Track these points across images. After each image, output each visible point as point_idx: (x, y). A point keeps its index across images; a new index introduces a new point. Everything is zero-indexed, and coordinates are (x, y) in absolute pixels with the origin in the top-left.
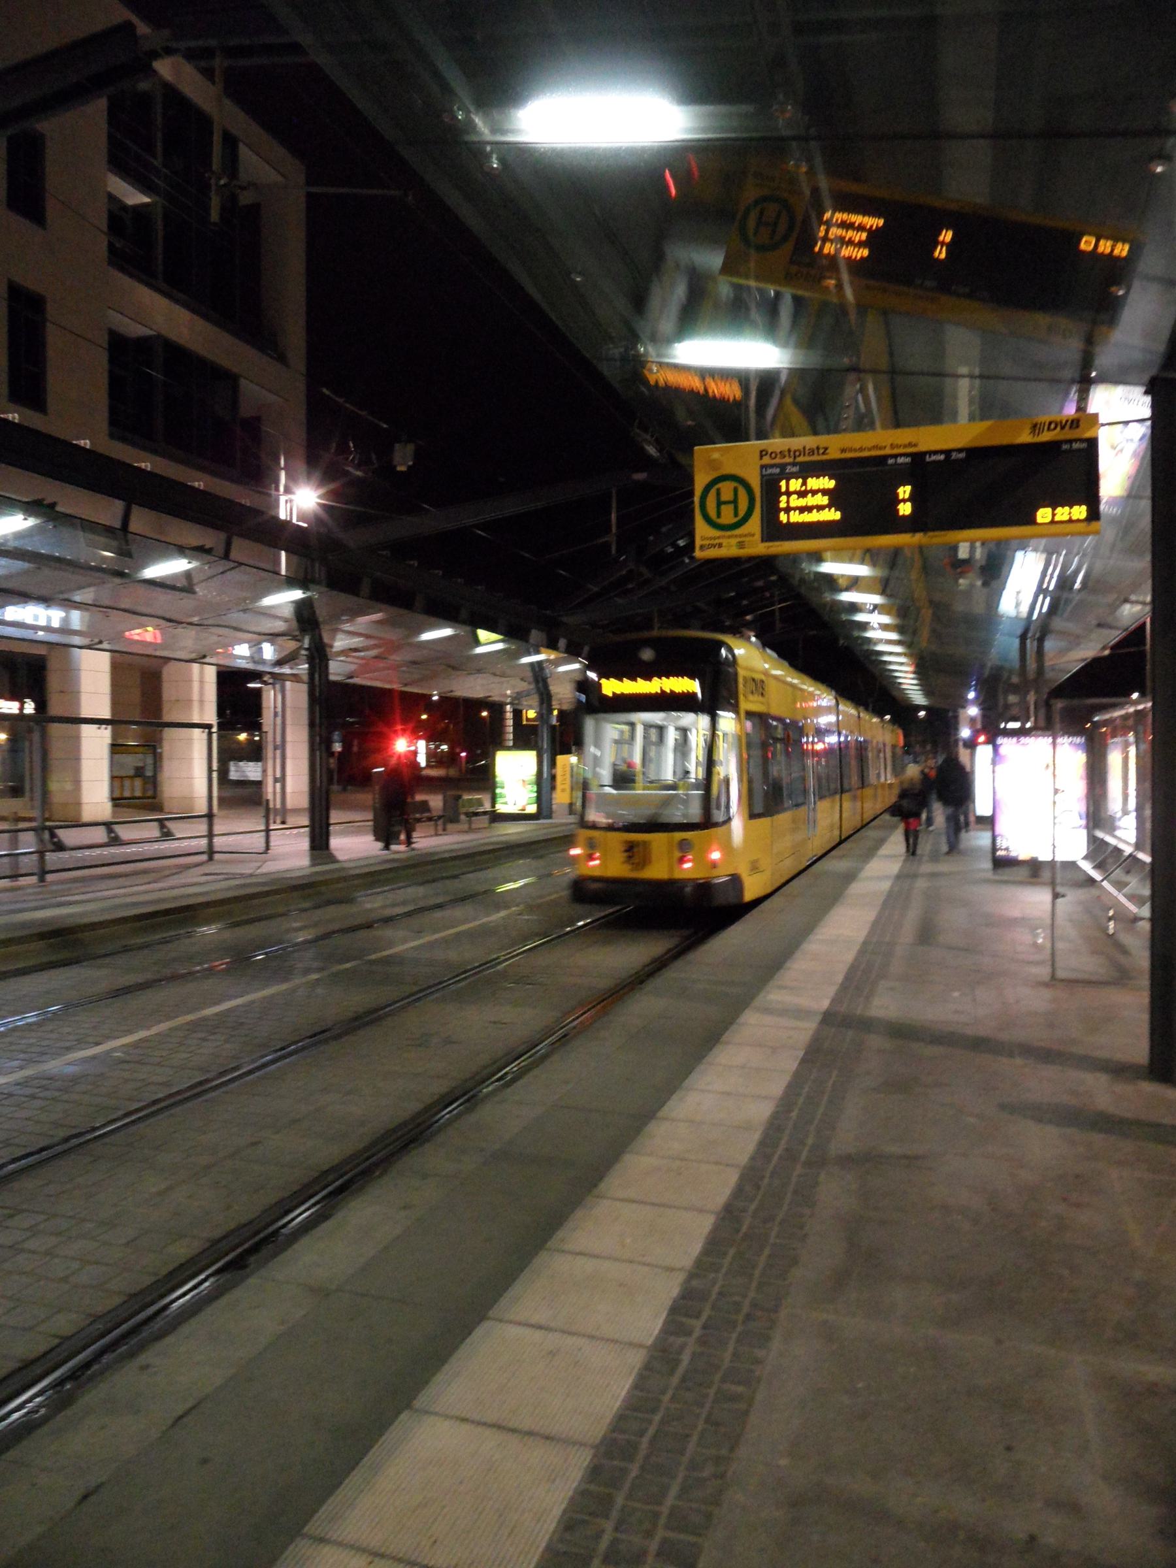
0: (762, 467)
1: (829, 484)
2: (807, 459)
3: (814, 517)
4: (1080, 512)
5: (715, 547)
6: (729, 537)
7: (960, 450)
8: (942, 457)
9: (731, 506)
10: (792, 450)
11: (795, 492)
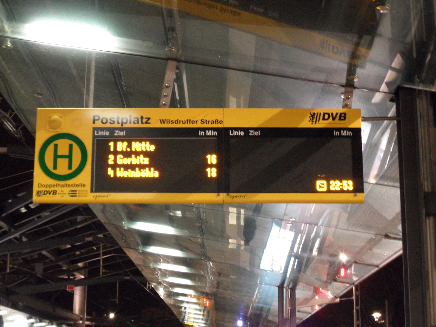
0: (94, 129)
1: (152, 148)
3: (136, 174)
4: (348, 185)
5: (50, 194)
6: (63, 186)
7: (256, 129)
8: (242, 133)
9: (66, 160)
11: (122, 153)
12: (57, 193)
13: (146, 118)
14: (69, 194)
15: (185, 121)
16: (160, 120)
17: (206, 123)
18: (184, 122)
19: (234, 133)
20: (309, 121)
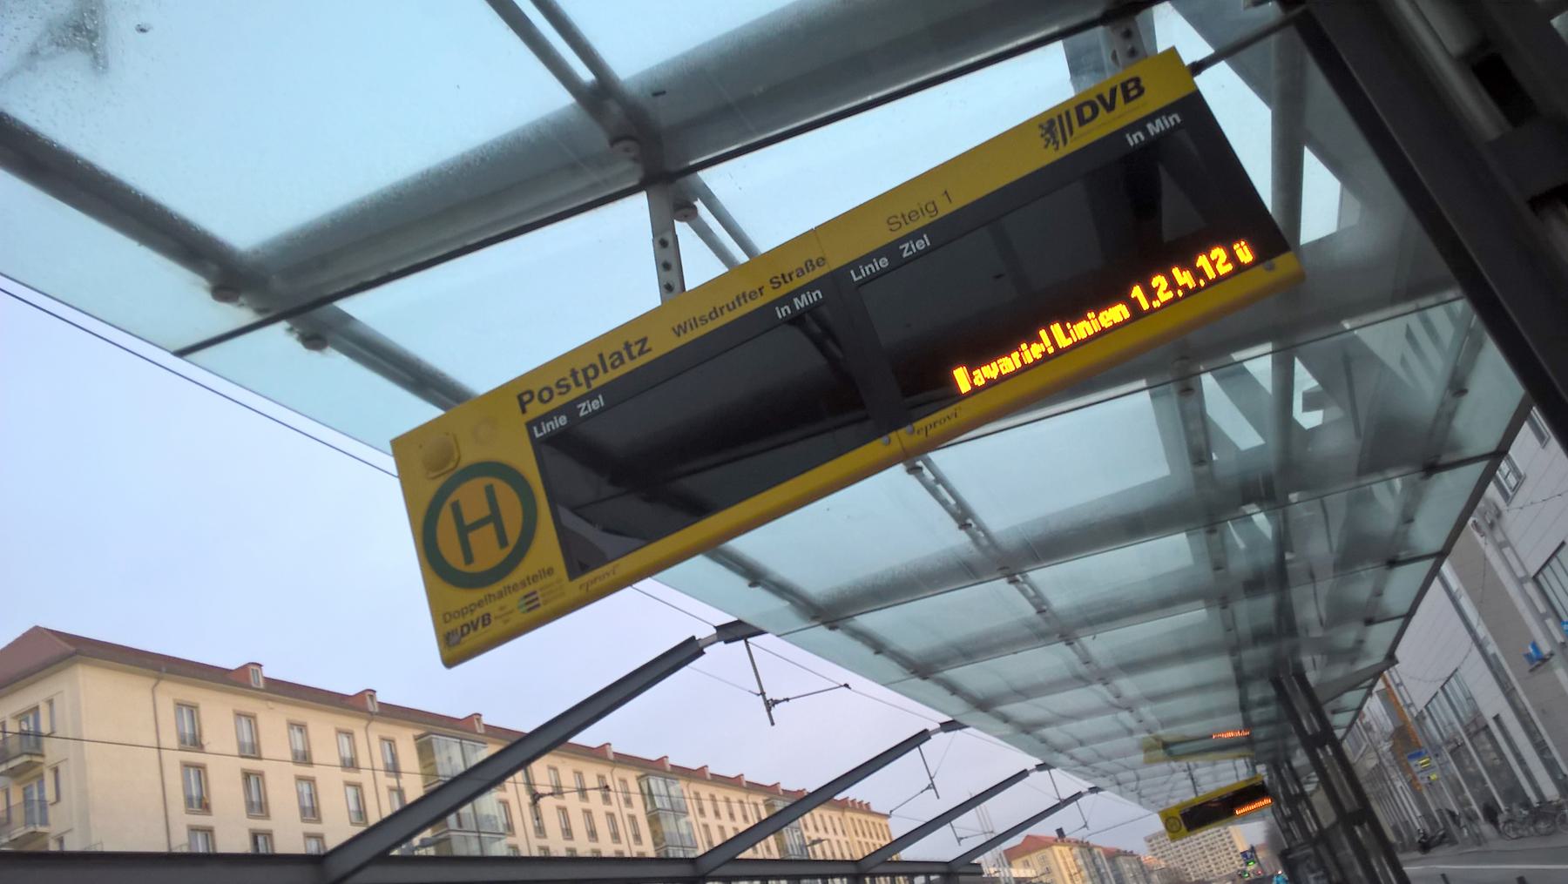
0: (529, 425)
2: (613, 374)
5: (475, 628)
6: (501, 595)
7: (915, 236)
10: (579, 368)
12: (492, 618)
13: (637, 343)
14: (519, 607)
15: (733, 303)
16: (674, 329)
17: (786, 282)
18: (731, 306)
19: (862, 271)
20: (1046, 146)
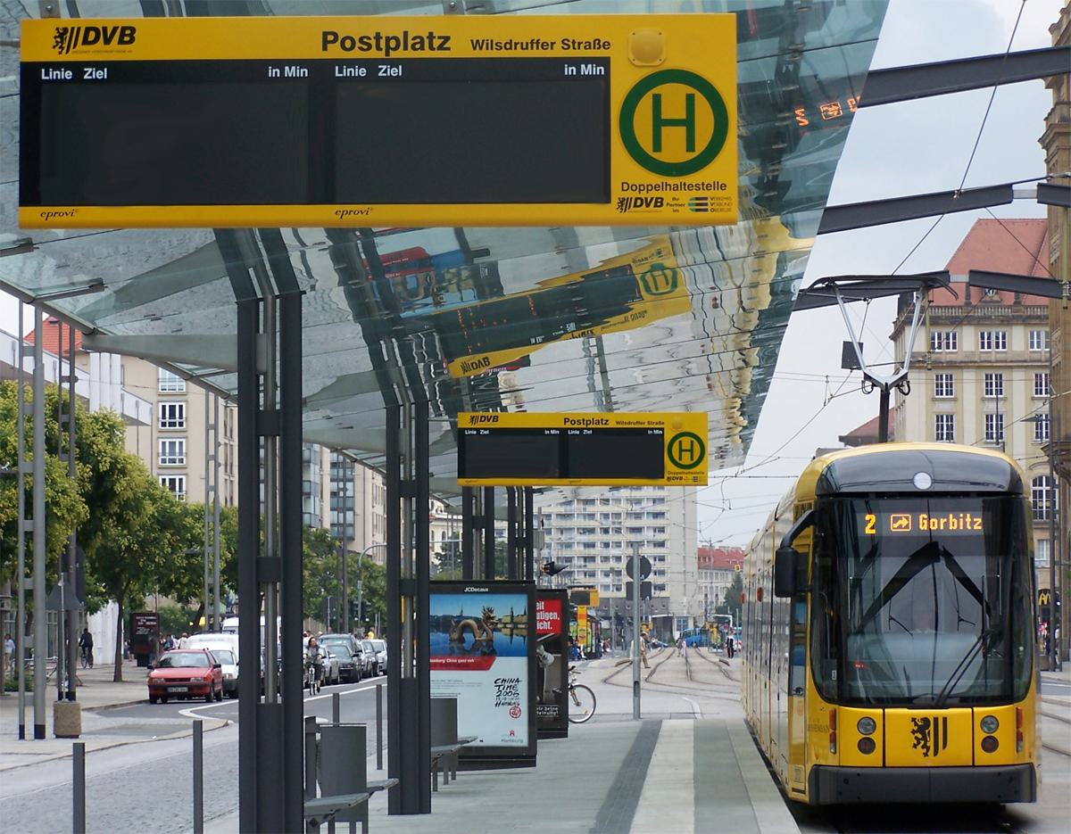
6: (676, 188)
13: (439, 38)
15: (527, 44)
16: (472, 41)
17: (574, 48)
